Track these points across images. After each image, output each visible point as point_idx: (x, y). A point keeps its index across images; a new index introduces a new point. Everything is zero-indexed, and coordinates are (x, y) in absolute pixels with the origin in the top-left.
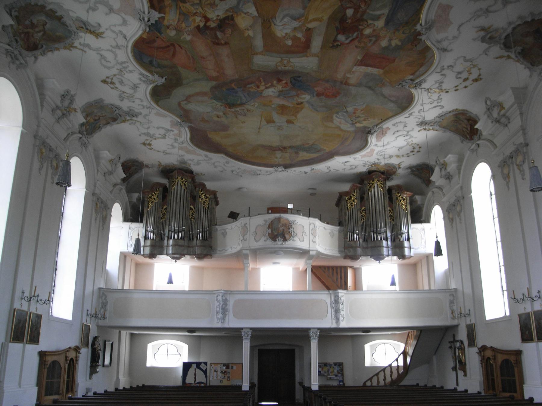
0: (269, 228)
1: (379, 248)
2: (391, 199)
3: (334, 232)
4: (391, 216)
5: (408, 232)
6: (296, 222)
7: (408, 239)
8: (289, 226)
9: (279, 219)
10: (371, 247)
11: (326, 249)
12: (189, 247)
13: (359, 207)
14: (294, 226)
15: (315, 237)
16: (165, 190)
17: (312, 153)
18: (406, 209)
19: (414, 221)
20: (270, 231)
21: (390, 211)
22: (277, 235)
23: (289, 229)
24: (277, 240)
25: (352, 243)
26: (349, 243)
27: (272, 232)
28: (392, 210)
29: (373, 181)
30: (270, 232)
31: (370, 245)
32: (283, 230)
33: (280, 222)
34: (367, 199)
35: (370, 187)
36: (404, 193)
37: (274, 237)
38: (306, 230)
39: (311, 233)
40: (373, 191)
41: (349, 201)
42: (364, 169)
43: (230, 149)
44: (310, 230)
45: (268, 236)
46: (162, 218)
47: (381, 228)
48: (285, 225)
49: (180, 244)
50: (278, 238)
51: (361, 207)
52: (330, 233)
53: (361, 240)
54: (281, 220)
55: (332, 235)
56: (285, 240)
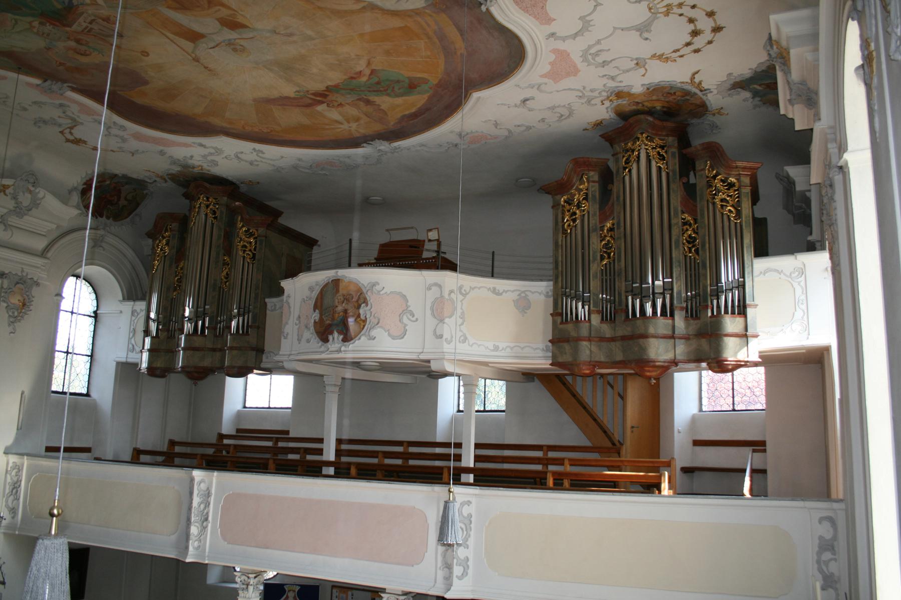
0: (315, 307)
1: (641, 341)
2: (690, 191)
3: (531, 297)
4: (691, 240)
5: (742, 286)
6: (378, 288)
7: (742, 309)
8: (359, 299)
9: (336, 282)
10: (624, 338)
11: (496, 348)
12: (214, 350)
13: (595, 221)
14: (371, 298)
15: (442, 321)
16: (184, 222)
17: (397, 96)
18: (739, 214)
19: (761, 251)
20: (316, 316)
21: (685, 223)
22: (330, 325)
23: (359, 307)
24: (330, 337)
25: (570, 327)
26: (561, 326)
27: (321, 315)
28: (696, 221)
29: (634, 143)
30: (317, 318)
31: (620, 332)
32: (346, 311)
33: (338, 291)
34: (618, 197)
35: (627, 162)
36: (730, 168)
37: (323, 333)
38: (415, 305)
39: (428, 312)
40: (634, 172)
41: (568, 207)
42: (603, 112)
43: (216, 121)
44: (429, 305)
45: (312, 328)
46: (175, 290)
47: (655, 277)
48: (347, 299)
49: (197, 345)
50: (332, 333)
51: (603, 220)
52: (516, 302)
53: (596, 319)
54: (342, 286)
55: (523, 305)
56: (347, 338)
